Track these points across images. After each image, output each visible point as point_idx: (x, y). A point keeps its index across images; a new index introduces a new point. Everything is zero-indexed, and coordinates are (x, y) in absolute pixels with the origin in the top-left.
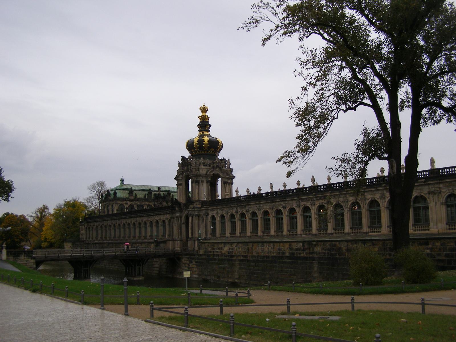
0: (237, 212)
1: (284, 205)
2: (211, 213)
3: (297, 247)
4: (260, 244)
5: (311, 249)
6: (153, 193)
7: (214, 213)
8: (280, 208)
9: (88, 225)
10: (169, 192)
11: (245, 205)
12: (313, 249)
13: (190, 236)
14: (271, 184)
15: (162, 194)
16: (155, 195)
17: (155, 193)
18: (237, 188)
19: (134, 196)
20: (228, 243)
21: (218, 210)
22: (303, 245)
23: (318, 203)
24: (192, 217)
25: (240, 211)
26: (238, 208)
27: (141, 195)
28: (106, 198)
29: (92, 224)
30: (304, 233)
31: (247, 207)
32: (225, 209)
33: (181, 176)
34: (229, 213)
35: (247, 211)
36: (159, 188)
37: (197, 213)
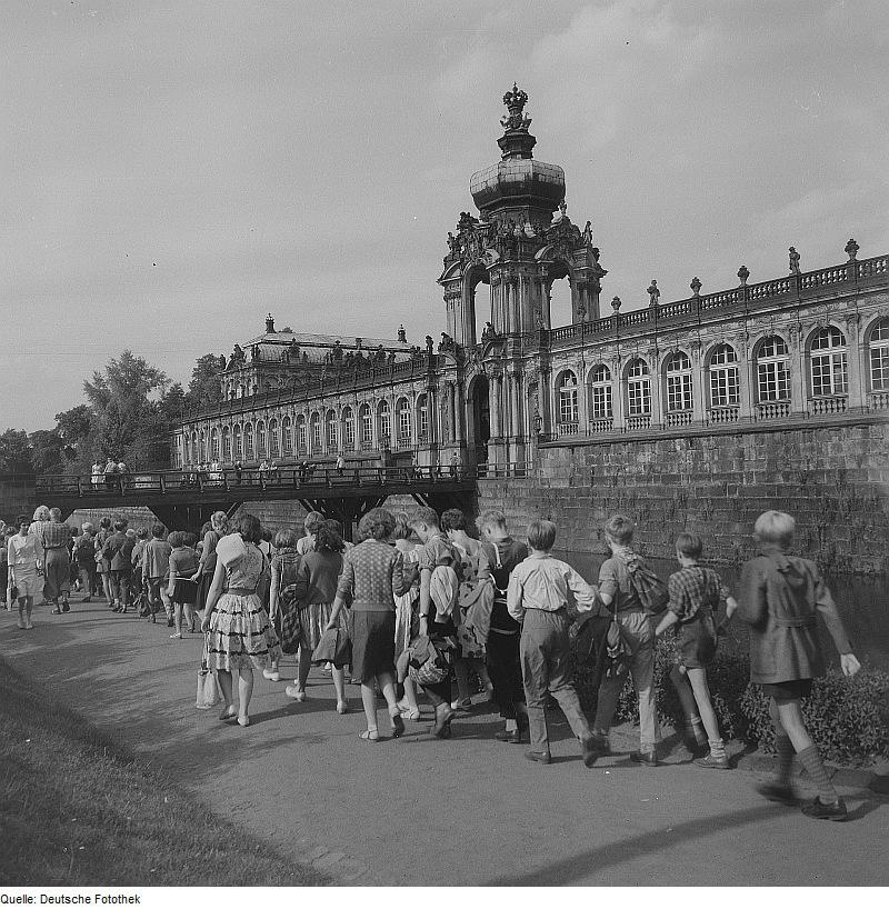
2: (557, 366)
6: (345, 351)
7: (571, 363)
8: (832, 323)
9: (192, 428)
10: (381, 351)
13: (494, 431)
14: (792, 249)
15: (365, 354)
16: (351, 355)
17: (349, 351)
18: (654, 282)
19: (301, 357)
20: (652, 440)
24: (500, 382)
26: (659, 339)
27: (317, 355)
28: (232, 363)
29: (201, 426)
31: (692, 336)
33: (457, 272)
35: (698, 344)
36: (359, 340)
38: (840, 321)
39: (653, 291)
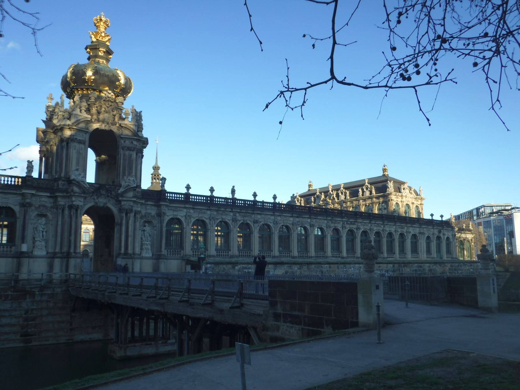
0: (235, 220)
1: (312, 223)
3: (387, 269)
4: (342, 266)
5: (401, 270)
8: (306, 226)
11: (253, 214)
12: (402, 270)
18: (234, 187)
21: (192, 211)
22: (393, 266)
23: (348, 227)
25: (239, 221)
30: (333, 255)
32: (209, 212)
34: (217, 219)
37: (139, 209)
38: (308, 225)
39: (233, 191)
